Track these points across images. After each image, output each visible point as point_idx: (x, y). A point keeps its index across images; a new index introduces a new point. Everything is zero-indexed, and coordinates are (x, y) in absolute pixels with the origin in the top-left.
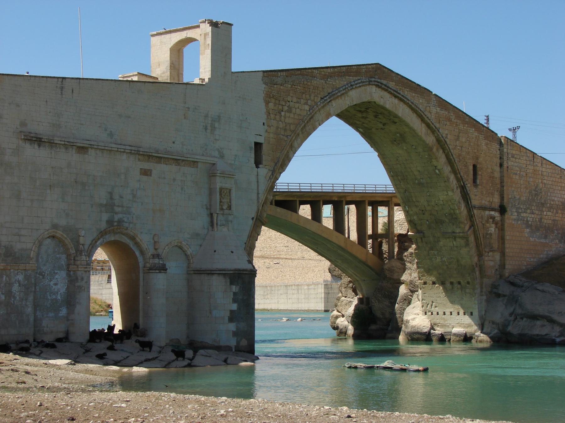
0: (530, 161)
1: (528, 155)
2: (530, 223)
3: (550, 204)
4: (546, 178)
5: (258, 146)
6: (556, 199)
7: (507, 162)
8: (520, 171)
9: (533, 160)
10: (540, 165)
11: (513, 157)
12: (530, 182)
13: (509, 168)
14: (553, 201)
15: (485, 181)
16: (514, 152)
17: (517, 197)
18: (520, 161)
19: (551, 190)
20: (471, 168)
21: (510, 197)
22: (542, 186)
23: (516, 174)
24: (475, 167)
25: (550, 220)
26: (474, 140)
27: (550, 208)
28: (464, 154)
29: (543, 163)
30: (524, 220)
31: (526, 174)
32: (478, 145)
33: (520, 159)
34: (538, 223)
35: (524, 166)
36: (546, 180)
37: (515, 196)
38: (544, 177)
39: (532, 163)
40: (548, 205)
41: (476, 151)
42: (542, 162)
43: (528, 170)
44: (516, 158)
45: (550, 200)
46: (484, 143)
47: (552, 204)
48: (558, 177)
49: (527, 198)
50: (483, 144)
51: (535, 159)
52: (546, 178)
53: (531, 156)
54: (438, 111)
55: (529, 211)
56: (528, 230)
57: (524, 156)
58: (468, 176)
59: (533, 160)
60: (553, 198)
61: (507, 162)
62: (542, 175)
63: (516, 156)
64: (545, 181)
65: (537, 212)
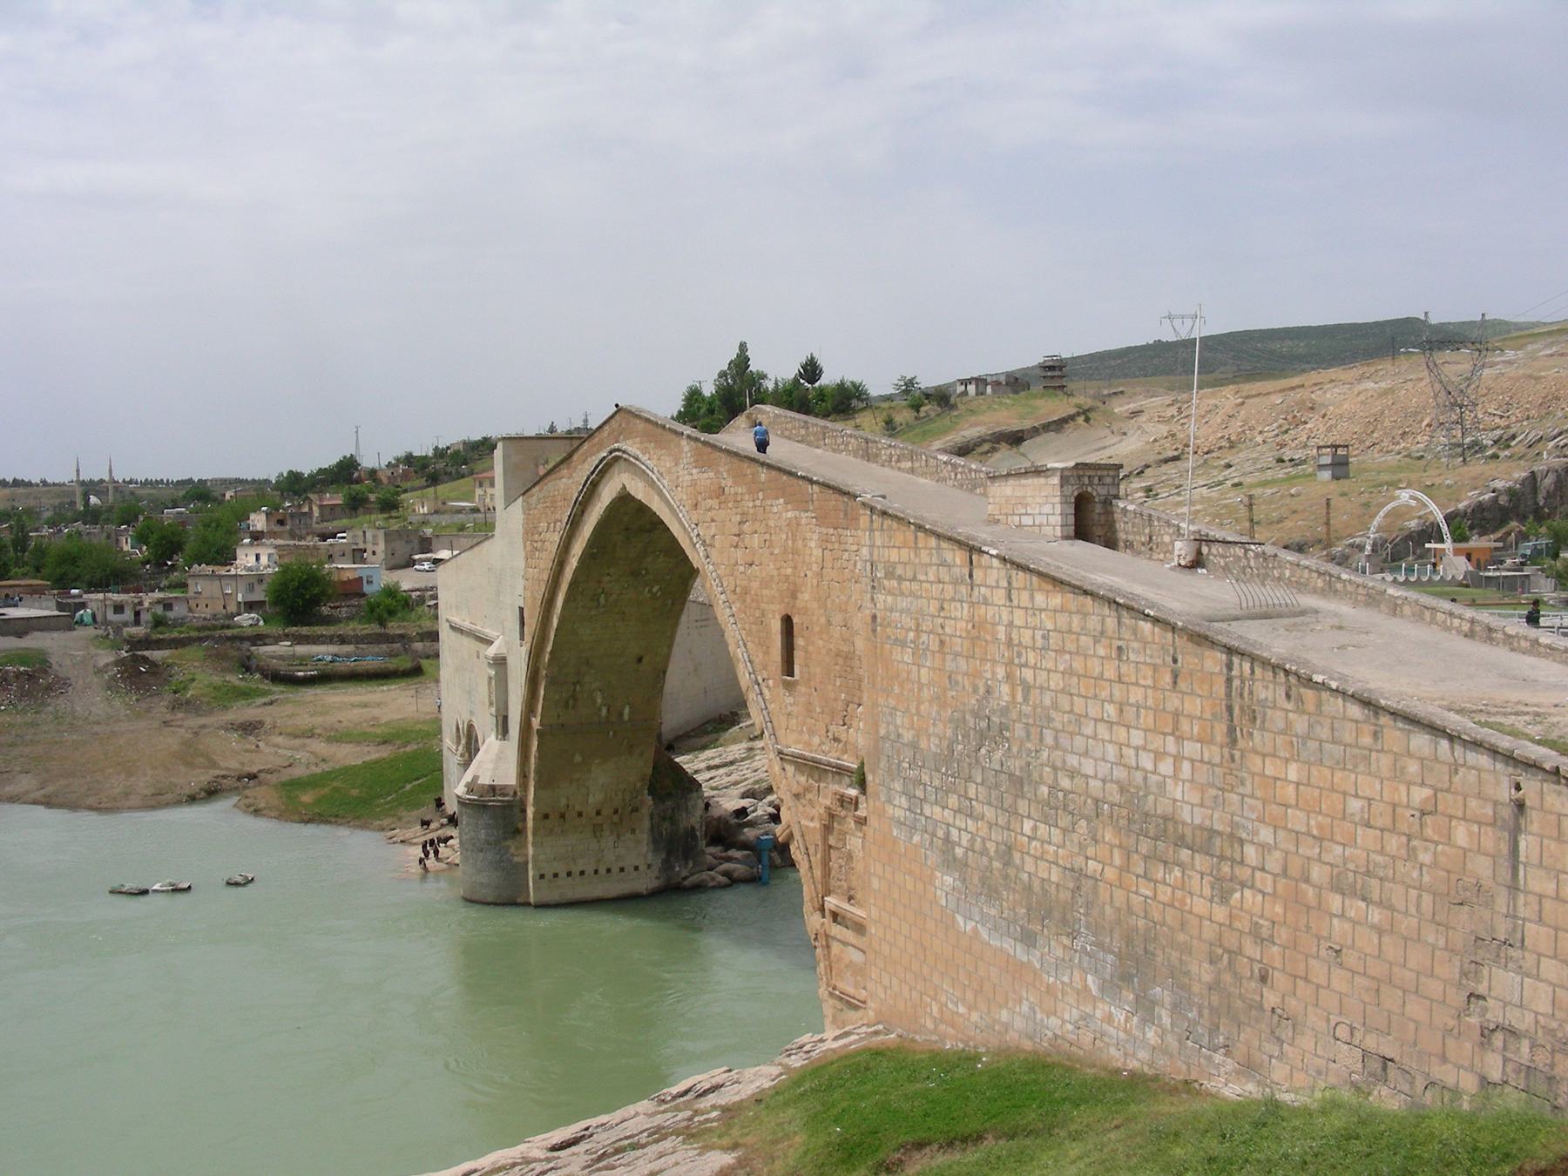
0: (956, 582)
1: (948, 556)
2: (959, 851)
3: (1053, 787)
4: (1031, 657)
5: (521, 610)
6: (1088, 767)
7: (873, 599)
8: (918, 630)
9: (971, 576)
10: (999, 596)
11: (890, 575)
12: (959, 678)
13: (879, 620)
14: (1073, 773)
15: (818, 670)
16: (894, 555)
17: (908, 736)
18: (915, 586)
19: (1059, 719)
20: (776, 626)
21: (882, 732)
22: (1013, 696)
23: (903, 645)
24: (787, 622)
25: (1054, 868)
26: (784, 537)
27: (1055, 808)
28: (755, 585)
29: (1015, 584)
30: (934, 835)
31: (942, 643)
32: (795, 552)
33: (914, 579)
34: (997, 864)
35: (933, 609)
36: (1035, 668)
37: (901, 731)
38: (1019, 655)
39: (963, 590)
40: (1044, 790)
41: (789, 571)
42: (1009, 583)
44: (900, 579)
45: (1055, 768)
46: (815, 537)
47: (1066, 793)
48: (1101, 652)
49: (945, 743)
50: (813, 544)
51: (975, 572)
52: (1031, 657)
53: (958, 561)
54: (695, 477)
55: (953, 800)
56: (948, 880)
57: (931, 565)
58: (767, 653)
59: (971, 576)
60: (1073, 761)
61: (873, 599)
62: (1010, 643)
63: (899, 571)
64: (1028, 674)
65: (989, 813)
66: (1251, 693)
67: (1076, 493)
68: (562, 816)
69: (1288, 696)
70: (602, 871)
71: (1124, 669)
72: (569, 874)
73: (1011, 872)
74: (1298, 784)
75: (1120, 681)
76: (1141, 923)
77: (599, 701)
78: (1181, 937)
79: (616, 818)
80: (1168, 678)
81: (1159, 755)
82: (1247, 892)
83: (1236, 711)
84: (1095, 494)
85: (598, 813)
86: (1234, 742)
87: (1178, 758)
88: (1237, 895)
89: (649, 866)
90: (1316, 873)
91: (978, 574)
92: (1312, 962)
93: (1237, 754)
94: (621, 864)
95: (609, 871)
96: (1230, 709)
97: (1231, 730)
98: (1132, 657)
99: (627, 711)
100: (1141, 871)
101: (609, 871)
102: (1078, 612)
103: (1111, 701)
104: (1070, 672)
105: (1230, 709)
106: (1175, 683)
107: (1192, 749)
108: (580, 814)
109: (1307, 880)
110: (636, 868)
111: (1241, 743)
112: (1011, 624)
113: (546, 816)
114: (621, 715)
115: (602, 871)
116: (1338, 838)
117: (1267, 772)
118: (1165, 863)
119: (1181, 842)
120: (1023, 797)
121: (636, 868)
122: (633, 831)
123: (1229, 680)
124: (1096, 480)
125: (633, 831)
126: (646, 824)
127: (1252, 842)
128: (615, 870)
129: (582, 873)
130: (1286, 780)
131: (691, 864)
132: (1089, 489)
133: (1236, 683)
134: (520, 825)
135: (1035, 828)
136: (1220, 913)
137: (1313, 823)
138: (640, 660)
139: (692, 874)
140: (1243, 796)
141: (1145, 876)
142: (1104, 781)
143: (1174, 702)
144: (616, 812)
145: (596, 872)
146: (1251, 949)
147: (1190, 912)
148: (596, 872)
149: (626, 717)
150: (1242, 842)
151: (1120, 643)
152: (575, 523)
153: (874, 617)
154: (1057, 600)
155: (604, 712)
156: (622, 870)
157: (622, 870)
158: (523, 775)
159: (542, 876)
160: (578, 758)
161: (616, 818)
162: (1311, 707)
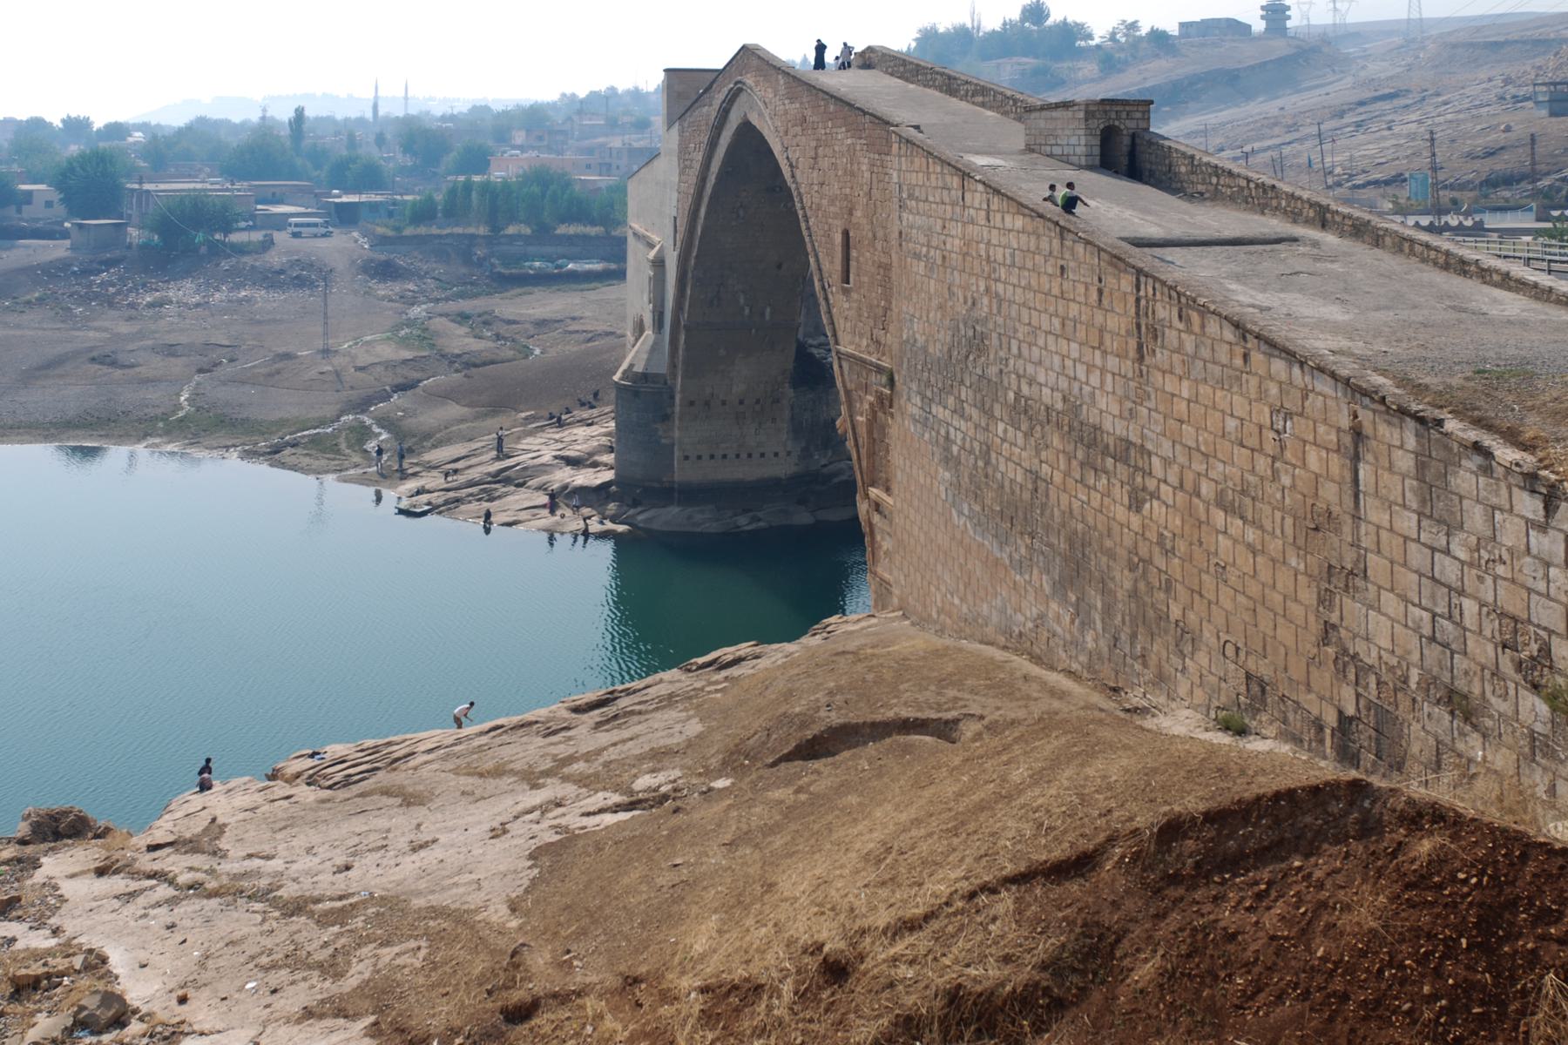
0: (953, 204)
2: (955, 449)
3: (1018, 394)
14: (1032, 381)
17: (921, 339)
19: (1022, 331)
20: (838, 238)
22: (990, 307)
24: (846, 234)
28: (825, 202)
29: (992, 207)
30: (938, 433)
31: (944, 257)
36: (1005, 283)
40: (1011, 395)
43: (949, 240)
45: (1019, 376)
48: (1050, 270)
49: (946, 349)
52: (1003, 272)
56: (947, 475)
57: (937, 188)
58: (832, 262)
60: (1030, 369)
64: (1000, 288)
65: (975, 413)
66: (1154, 312)
67: (1102, 126)
68: (707, 404)
69: (1180, 317)
70: (744, 456)
71: (1066, 285)
72: (712, 457)
73: (990, 471)
74: (1189, 401)
75: (1063, 298)
76: (1080, 527)
77: (742, 301)
78: (1108, 543)
79: (758, 407)
80: (1095, 296)
81: (1090, 368)
82: (1155, 503)
83: (1143, 329)
84: (1122, 127)
85: (741, 402)
86: (1141, 358)
87: (1103, 371)
88: (1147, 506)
89: (789, 453)
90: (1206, 489)
91: (968, 196)
92: (1204, 577)
93: (1144, 369)
94: (762, 450)
95: (750, 456)
96: (1139, 326)
97: (1140, 347)
98: (1071, 276)
99: (768, 310)
100: (1078, 477)
101: (750, 456)
102: (1034, 233)
103: (1057, 316)
104: (1028, 287)
105: (1139, 326)
106: (1100, 300)
107: (1112, 362)
108: (724, 403)
109: (1199, 495)
110: (776, 454)
111: (1148, 360)
112: (989, 243)
113: (692, 403)
114: (763, 314)
115: (744, 456)
116: (1220, 455)
117: (1167, 389)
118: (1096, 470)
119: (1105, 452)
120: (997, 401)
121: (776, 454)
122: (774, 420)
123: (1138, 300)
124: (1124, 115)
125: (774, 420)
126: (787, 414)
127: (1156, 454)
128: (756, 455)
129: (724, 456)
130: (1180, 397)
131: (830, 453)
132: (1117, 123)
133: (1143, 302)
134: (669, 411)
135: (1005, 431)
136: (1135, 521)
137: (1201, 439)
138: (779, 266)
139: (831, 463)
140: (1150, 410)
141: (1081, 482)
142: (1052, 390)
143: (1099, 318)
144: (758, 402)
145: (738, 456)
146: (1160, 561)
147: (1114, 519)
148: (738, 456)
149: (768, 317)
150: (1150, 454)
151: (1062, 262)
152: (713, 144)
153: (901, 233)
154: (1019, 222)
155: (747, 311)
156: (762, 455)
157: (762, 455)
158: (673, 366)
159: (687, 458)
160: (722, 352)
161: (758, 407)
162: (1196, 328)
